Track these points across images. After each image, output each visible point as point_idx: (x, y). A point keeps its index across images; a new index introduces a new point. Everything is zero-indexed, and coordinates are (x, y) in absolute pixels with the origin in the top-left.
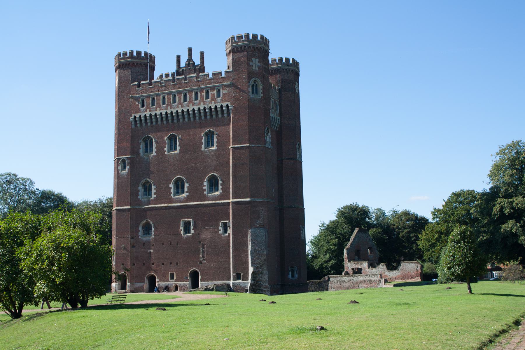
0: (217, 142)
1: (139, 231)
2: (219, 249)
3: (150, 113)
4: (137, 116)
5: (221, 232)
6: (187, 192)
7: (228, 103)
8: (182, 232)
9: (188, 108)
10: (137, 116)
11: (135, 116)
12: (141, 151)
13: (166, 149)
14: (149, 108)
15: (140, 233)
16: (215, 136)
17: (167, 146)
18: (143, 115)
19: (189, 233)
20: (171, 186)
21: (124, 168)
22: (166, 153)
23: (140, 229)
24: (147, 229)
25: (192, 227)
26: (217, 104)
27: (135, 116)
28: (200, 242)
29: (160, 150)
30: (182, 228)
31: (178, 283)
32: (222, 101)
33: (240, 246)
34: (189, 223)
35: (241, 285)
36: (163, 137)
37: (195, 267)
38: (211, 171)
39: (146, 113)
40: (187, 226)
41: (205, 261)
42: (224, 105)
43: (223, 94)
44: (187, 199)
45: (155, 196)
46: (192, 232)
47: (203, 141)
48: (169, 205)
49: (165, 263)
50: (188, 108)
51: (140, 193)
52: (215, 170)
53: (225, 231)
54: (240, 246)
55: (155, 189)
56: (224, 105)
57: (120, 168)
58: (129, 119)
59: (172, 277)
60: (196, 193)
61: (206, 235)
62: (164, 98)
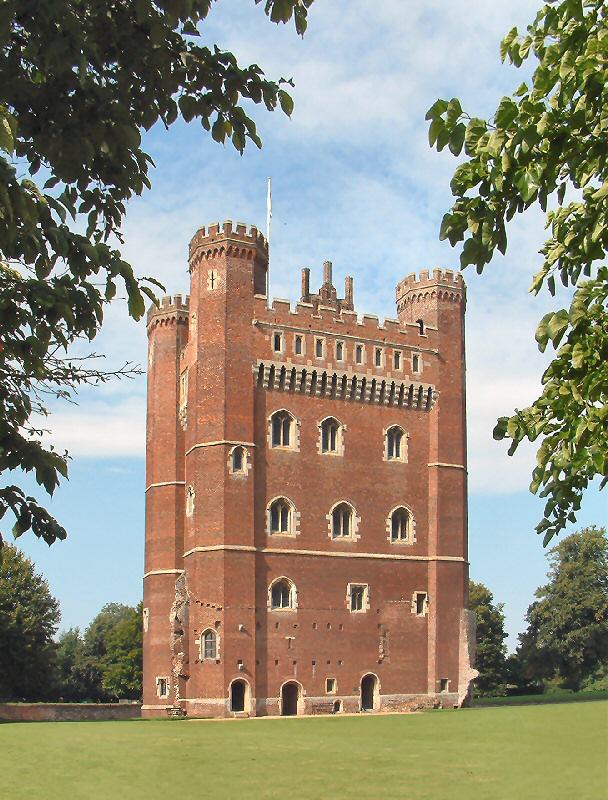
0: (410, 451)
1: (267, 599)
2: (415, 639)
3: (294, 365)
4: (268, 364)
5: (414, 610)
6: (356, 533)
7: (430, 385)
8: (349, 607)
9: (365, 375)
10: (268, 364)
11: (262, 367)
12: (270, 438)
13: (319, 445)
14: (291, 355)
15: (269, 603)
16: (404, 439)
17: (321, 438)
18: (278, 366)
19: (360, 608)
20: (330, 517)
21: (238, 465)
22: (320, 452)
23: (270, 594)
24: (281, 592)
25: (365, 599)
26: (414, 383)
27: (262, 367)
28: (379, 626)
29: (307, 442)
30: (349, 599)
31: (342, 699)
32: (423, 378)
33: (447, 638)
34: (361, 590)
35: (449, 699)
36: (312, 421)
37: (371, 668)
38: (397, 501)
39: (284, 364)
40: (357, 593)
41: (387, 660)
42: (426, 387)
43: (425, 368)
44: (360, 546)
45: (299, 533)
46: (365, 606)
47: (386, 443)
48: (328, 553)
49: (318, 662)
50: (365, 375)
51: (268, 523)
52: (406, 498)
53: (419, 610)
54: (447, 638)
55: (298, 519)
56: (426, 387)
57: (230, 463)
58: (249, 366)
59: (330, 689)
60: (372, 536)
61: (390, 614)
62: (319, 342)
